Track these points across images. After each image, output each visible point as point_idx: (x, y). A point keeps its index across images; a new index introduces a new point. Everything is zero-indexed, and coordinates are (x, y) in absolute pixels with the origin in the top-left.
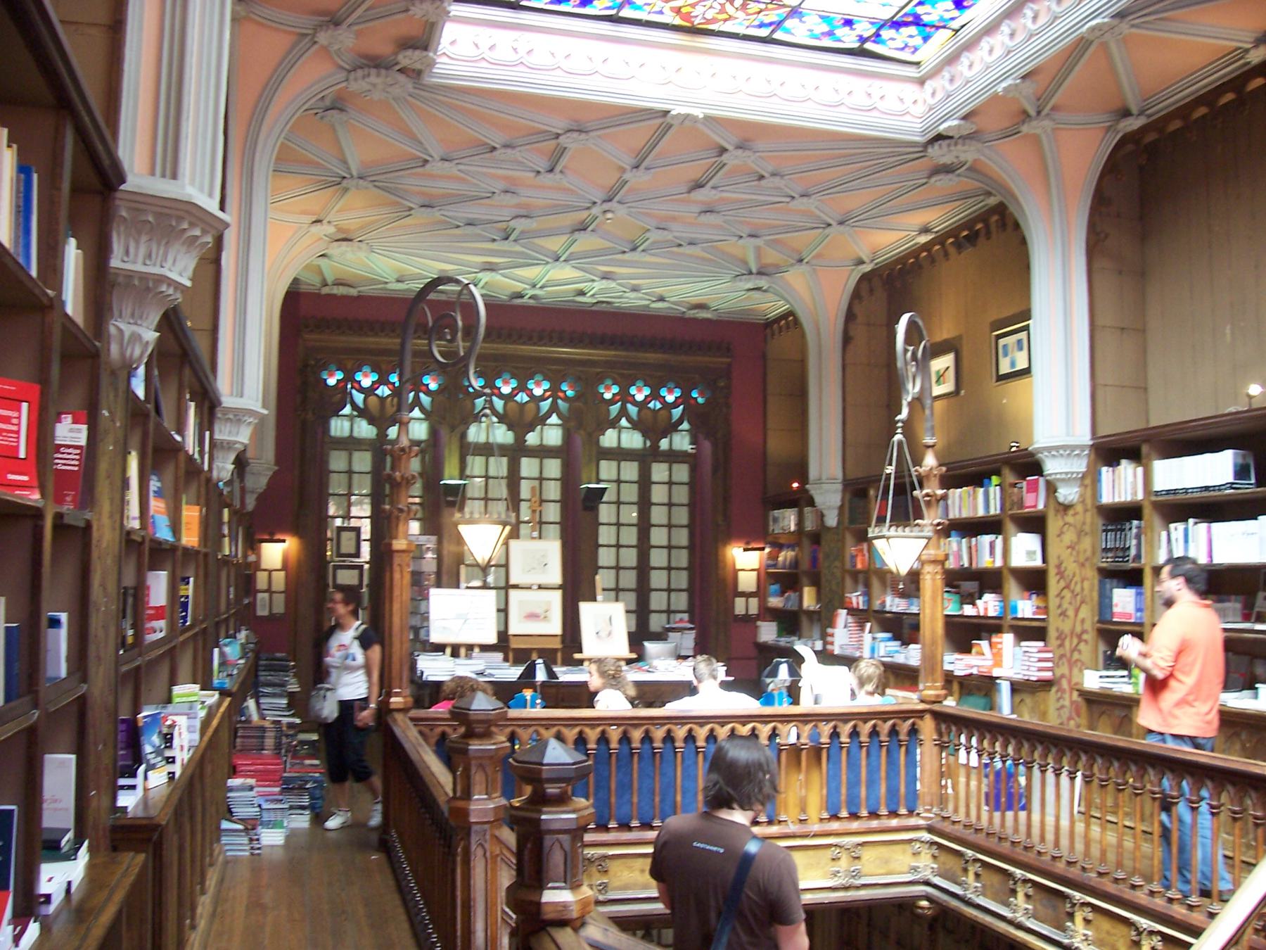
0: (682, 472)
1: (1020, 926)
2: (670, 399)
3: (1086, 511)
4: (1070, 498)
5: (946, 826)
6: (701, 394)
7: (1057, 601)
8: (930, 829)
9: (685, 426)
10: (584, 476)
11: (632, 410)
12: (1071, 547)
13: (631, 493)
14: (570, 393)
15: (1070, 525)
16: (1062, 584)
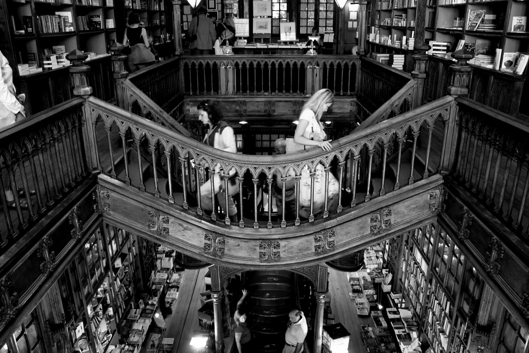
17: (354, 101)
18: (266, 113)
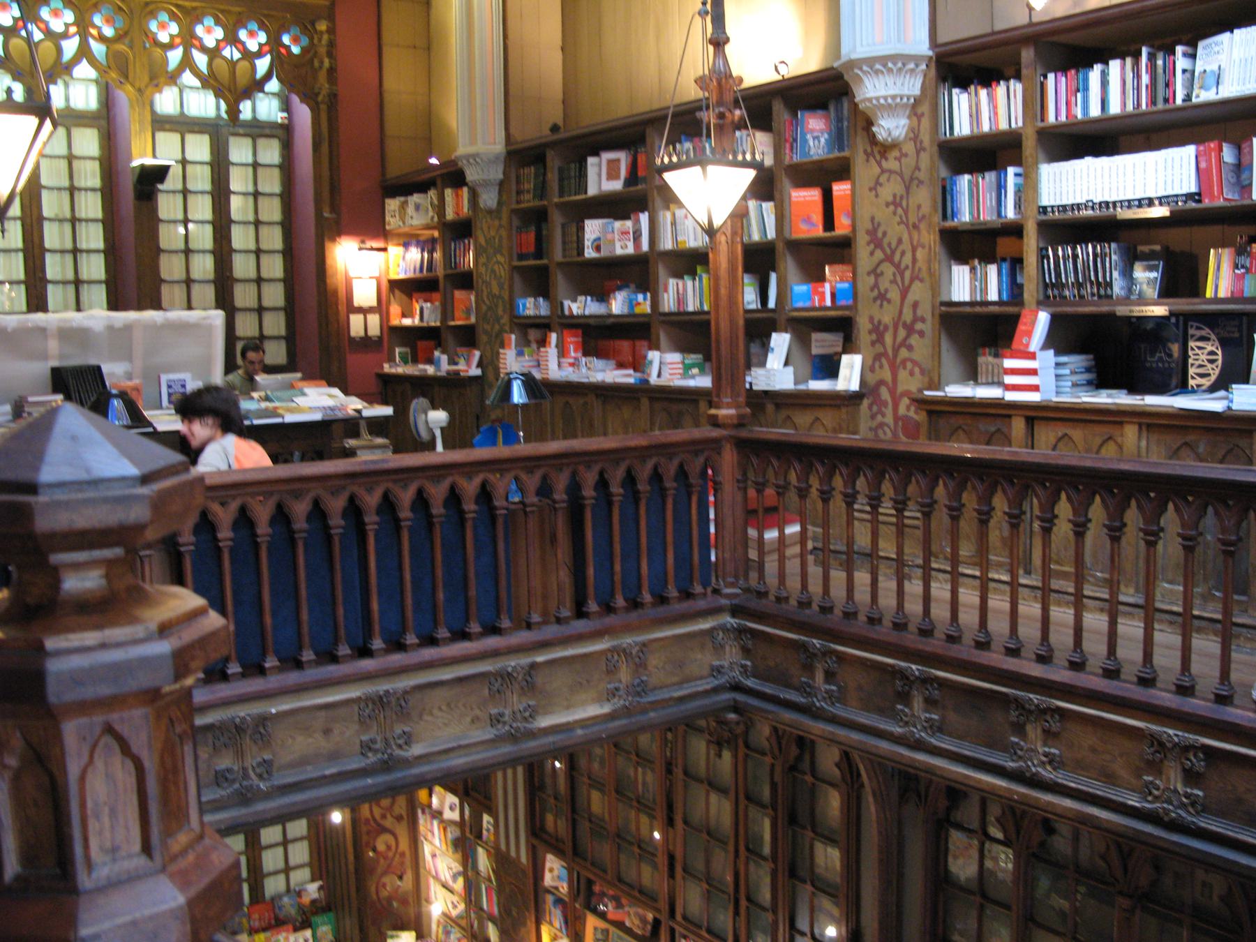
0: (271, 153)
1: (919, 746)
2: (253, 46)
3: (919, 150)
4: (896, 133)
5: (754, 604)
6: (295, 40)
7: (872, 279)
8: (736, 611)
9: (273, 85)
10: (135, 151)
11: (201, 60)
12: (896, 203)
13: (201, 179)
14: (109, 32)
15: (891, 172)
16: (879, 255)
17: (723, 628)
18: (372, 758)
